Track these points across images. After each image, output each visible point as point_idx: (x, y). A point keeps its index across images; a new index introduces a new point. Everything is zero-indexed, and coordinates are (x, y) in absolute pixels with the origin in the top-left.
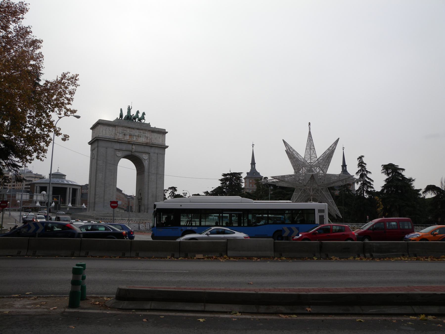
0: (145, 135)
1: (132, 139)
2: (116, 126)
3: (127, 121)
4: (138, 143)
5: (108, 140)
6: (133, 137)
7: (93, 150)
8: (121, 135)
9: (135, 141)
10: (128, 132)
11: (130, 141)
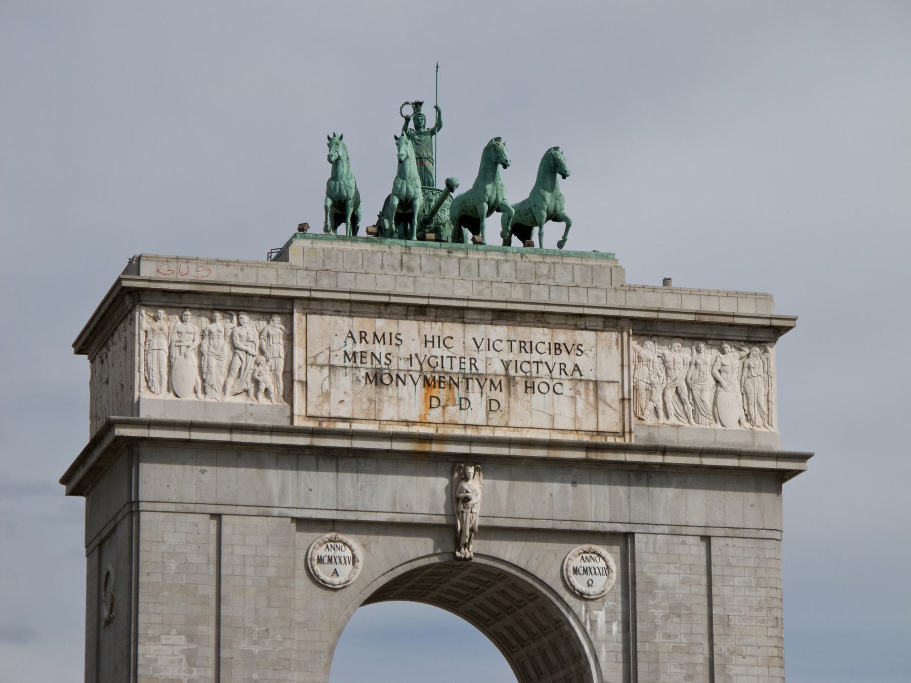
0: (563, 357)
1: (452, 410)
2: (292, 299)
3: (394, 248)
4: (510, 443)
5: (224, 437)
6: (459, 392)
7: (100, 545)
9: (486, 433)
11: (430, 430)
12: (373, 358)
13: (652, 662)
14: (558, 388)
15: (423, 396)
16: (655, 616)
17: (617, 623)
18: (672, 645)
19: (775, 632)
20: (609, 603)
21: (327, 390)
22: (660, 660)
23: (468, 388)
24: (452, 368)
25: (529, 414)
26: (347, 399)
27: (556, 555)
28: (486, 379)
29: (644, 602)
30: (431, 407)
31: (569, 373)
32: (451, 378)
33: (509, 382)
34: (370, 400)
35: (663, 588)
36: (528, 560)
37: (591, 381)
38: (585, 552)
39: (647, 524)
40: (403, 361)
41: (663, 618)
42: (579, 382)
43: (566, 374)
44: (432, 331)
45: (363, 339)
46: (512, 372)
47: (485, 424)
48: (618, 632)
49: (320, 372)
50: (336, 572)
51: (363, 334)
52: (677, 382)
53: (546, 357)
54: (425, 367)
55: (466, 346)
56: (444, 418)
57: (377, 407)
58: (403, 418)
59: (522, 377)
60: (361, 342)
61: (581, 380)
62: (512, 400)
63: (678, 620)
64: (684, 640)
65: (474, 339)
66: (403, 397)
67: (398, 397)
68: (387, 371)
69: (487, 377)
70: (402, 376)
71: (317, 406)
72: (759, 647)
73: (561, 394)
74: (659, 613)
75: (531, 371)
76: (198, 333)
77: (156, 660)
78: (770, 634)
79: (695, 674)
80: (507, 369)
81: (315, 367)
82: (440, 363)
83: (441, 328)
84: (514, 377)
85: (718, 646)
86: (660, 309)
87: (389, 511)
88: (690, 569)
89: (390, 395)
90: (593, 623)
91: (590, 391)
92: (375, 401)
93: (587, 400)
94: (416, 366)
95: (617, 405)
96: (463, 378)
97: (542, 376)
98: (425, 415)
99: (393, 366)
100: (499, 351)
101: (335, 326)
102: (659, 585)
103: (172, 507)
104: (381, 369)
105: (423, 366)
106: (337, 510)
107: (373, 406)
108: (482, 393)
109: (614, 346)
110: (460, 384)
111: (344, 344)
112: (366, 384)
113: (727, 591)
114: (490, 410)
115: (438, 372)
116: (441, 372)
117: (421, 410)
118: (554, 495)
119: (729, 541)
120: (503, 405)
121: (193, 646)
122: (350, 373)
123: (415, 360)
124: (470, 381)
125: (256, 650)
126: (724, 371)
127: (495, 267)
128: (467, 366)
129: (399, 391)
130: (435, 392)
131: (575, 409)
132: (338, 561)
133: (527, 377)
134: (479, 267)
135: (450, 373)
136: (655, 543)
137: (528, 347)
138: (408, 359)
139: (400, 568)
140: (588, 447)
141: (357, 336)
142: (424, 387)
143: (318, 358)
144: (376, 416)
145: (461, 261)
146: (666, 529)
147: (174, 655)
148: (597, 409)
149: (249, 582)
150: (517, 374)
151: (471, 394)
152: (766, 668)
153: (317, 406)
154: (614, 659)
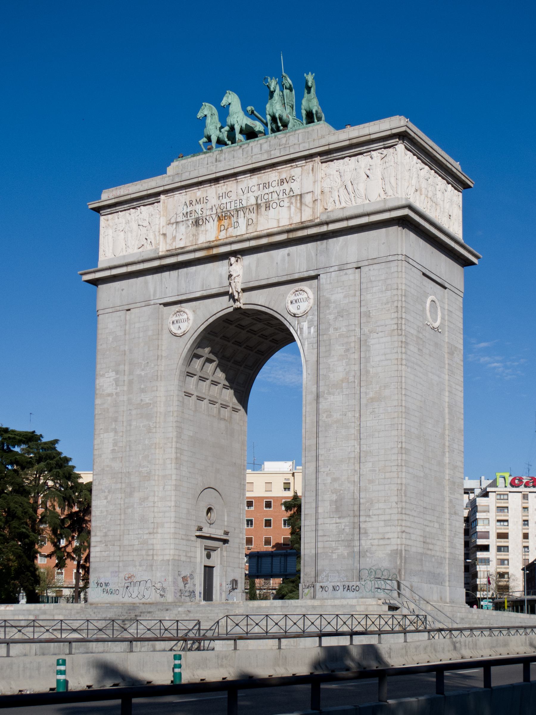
0: (286, 186)
1: (230, 230)
8: (182, 228)
10: (213, 201)
14: (282, 204)
19: (396, 315)
20: (310, 317)
25: (266, 221)
26: (183, 237)
27: (283, 296)
31: (287, 194)
32: (230, 213)
33: (258, 207)
34: (193, 235)
35: (334, 302)
37: (298, 195)
38: (297, 291)
40: (208, 210)
42: (292, 198)
46: (259, 202)
51: (191, 201)
52: (345, 183)
53: (277, 189)
54: (219, 211)
57: (197, 238)
58: (208, 240)
59: (264, 203)
61: (293, 196)
62: (259, 216)
63: (342, 319)
64: (345, 330)
68: (201, 218)
70: (208, 218)
72: (386, 326)
74: (331, 317)
75: (268, 199)
76: (124, 222)
77: (103, 386)
78: (392, 317)
80: (257, 201)
81: (170, 225)
82: (225, 207)
84: (260, 204)
89: (202, 230)
90: (301, 329)
93: (296, 207)
94: (214, 212)
95: (311, 205)
99: (204, 215)
102: (332, 301)
103: (110, 310)
104: (198, 218)
107: (194, 238)
109: (311, 172)
113: (369, 297)
119: (371, 267)
120: (254, 220)
121: (118, 376)
123: (214, 209)
124: (239, 212)
125: (143, 373)
127: (260, 148)
128: (238, 204)
132: (182, 321)
133: (266, 202)
134: (252, 150)
136: (330, 277)
137: (267, 186)
139: (210, 319)
140: (288, 231)
146: (336, 268)
147: (110, 382)
148: (301, 210)
150: (262, 202)
151: (239, 219)
152: (390, 337)
154: (312, 347)
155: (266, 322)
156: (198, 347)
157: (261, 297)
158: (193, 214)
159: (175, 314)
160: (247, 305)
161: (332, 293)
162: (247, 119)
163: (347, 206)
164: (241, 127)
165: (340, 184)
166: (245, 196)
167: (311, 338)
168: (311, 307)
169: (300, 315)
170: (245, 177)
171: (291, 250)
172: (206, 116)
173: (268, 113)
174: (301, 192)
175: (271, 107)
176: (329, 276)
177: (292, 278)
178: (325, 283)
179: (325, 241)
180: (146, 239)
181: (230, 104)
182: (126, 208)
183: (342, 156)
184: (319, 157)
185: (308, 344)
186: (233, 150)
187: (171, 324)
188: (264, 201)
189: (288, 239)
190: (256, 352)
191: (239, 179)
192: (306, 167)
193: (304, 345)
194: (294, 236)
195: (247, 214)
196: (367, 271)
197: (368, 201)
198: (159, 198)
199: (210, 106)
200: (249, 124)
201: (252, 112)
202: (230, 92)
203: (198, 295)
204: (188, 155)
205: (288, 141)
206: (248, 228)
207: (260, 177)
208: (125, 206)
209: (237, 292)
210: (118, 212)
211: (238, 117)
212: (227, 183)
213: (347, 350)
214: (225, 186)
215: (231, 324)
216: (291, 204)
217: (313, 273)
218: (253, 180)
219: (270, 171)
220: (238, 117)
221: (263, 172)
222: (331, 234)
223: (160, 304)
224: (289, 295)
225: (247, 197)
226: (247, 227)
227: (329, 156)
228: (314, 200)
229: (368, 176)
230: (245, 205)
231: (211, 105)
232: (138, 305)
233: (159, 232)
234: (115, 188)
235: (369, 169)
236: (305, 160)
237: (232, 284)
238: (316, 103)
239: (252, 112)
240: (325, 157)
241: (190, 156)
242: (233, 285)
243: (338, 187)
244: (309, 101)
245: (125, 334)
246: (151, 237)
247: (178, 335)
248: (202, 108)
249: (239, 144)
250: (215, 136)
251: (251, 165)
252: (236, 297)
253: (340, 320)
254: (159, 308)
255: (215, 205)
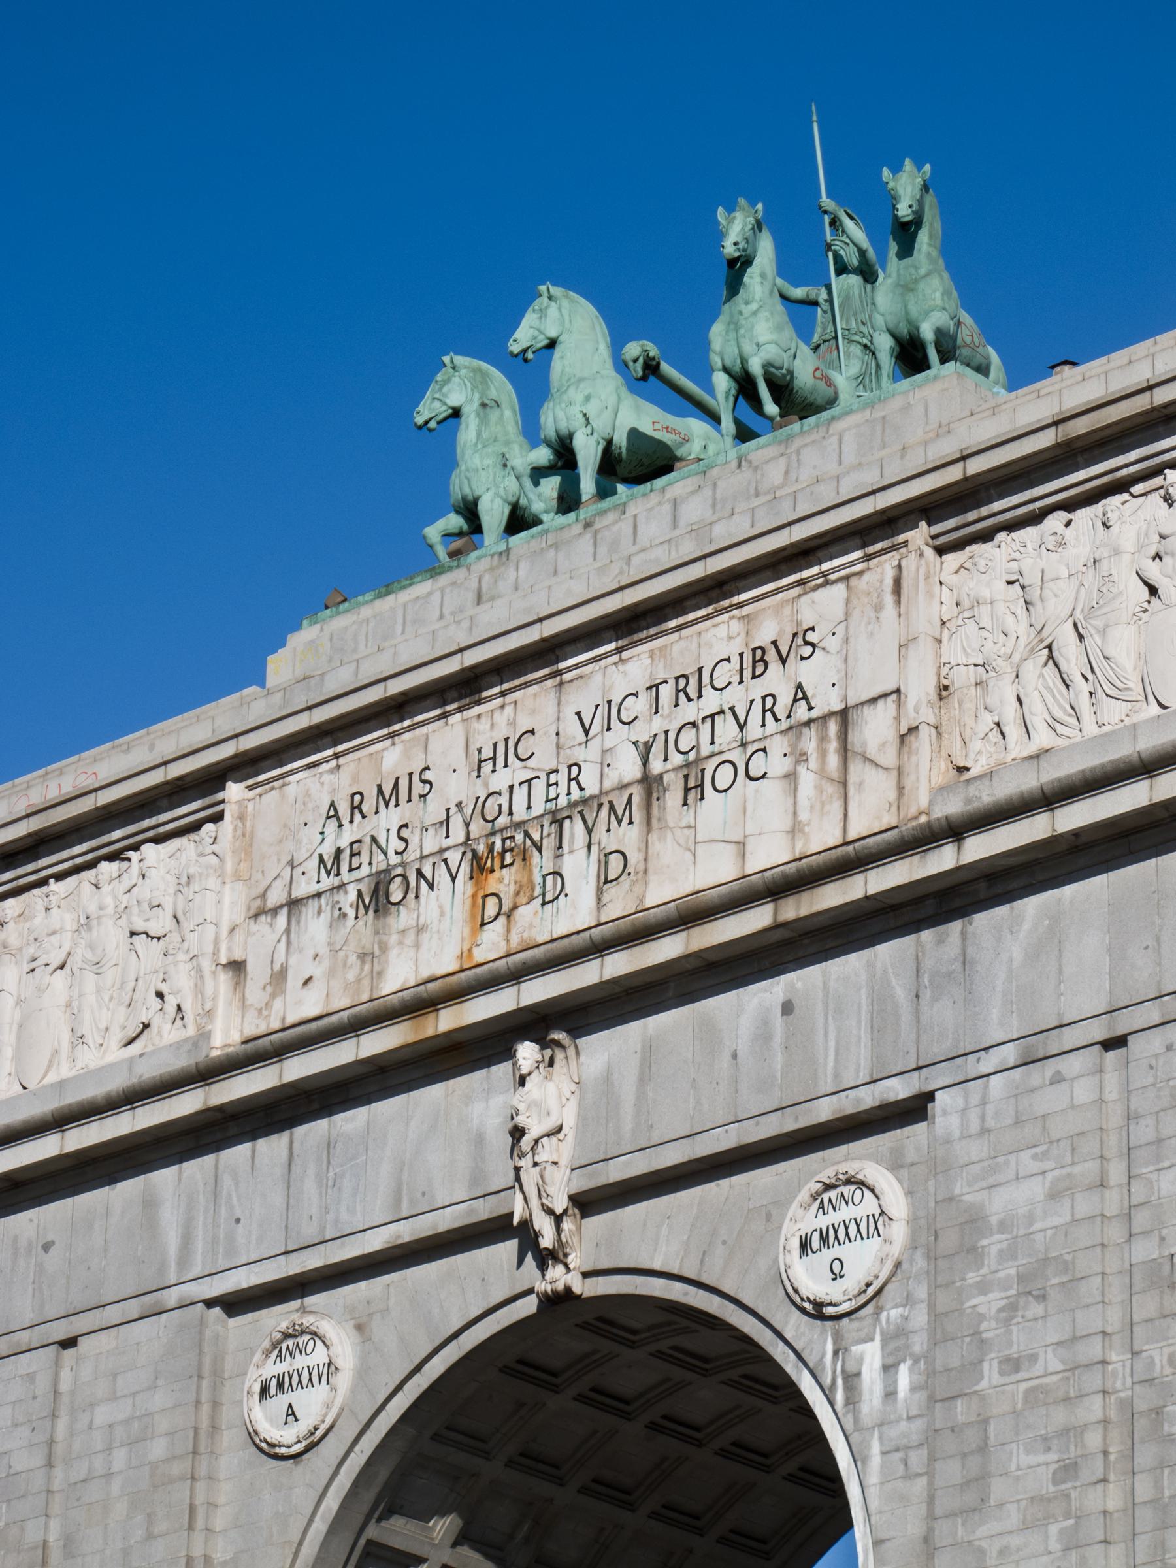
0: (777, 681)
1: (526, 913)
12: (374, 846)
13: (972, 1452)
15: (469, 902)
16: (980, 1314)
17: (909, 1362)
18: (1023, 1386)
20: (892, 1314)
21: (282, 964)
22: (992, 1441)
23: (560, 847)
24: (529, 808)
25: (688, 855)
26: (317, 971)
27: (768, 1217)
28: (600, 805)
29: (953, 1283)
30: (483, 924)
31: (781, 715)
33: (648, 794)
34: (363, 956)
35: (1003, 1227)
36: (704, 1253)
37: (832, 714)
38: (828, 1187)
39: (962, 1056)
40: (431, 831)
41: (1004, 1314)
42: (805, 730)
43: (777, 720)
44: (494, 734)
45: (356, 811)
47: (593, 924)
48: (913, 1389)
49: (271, 925)
50: (291, 1412)
51: (357, 798)
52: (1045, 633)
53: (736, 696)
55: (562, 740)
56: (508, 941)
57: (377, 968)
60: (351, 821)
61: (808, 723)
62: (653, 837)
65: (578, 714)
66: (429, 923)
67: (417, 926)
68: (399, 870)
69: (605, 800)
71: (260, 1011)
73: (764, 776)
74: (989, 1303)
79: (1082, 1456)
80: (645, 762)
81: (262, 918)
82: (505, 808)
83: (512, 716)
84: (661, 776)
85: (1144, 1354)
86: (965, 453)
87: (387, 1221)
88: (1073, 1149)
89: (401, 928)
90: (852, 1379)
91: (829, 742)
92: (373, 953)
93: (822, 773)
94: (458, 834)
95: (889, 758)
96: (551, 823)
97: (724, 747)
98: (470, 950)
99: (412, 855)
100: (629, 723)
101: (304, 804)
102: (994, 1220)
104: (387, 871)
105: (472, 827)
106: (286, 1253)
107: (367, 967)
108: (589, 846)
109: (889, 599)
110: (545, 842)
111: (320, 837)
112: (356, 918)
114: (606, 882)
115: (501, 830)
116: (506, 828)
117: (463, 940)
118: (740, 1054)
120: (634, 857)
122: (327, 905)
123: (457, 823)
124: (567, 823)
126: (1166, 554)
127: (669, 518)
129: (422, 910)
130: (492, 883)
131: (795, 803)
132: (305, 1381)
133: (688, 765)
135: (524, 822)
136: (984, 1103)
137: (692, 690)
138: (441, 823)
141: (344, 809)
142: (471, 878)
143: (269, 893)
144: (372, 990)
145: (599, 537)
146: (1009, 1054)
148: (845, 784)
149: (116, 1487)
150: (669, 766)
151: (566, 858)
153: (260, 1011)
154: (901, 1469)
155: (734, 1374)
156: (389, 1512)
157: (664, 1230)
158: (364, 857)
159: (276, 1345)
160: (601, 1279)
161: (991, 1181)
162: (638, 408)
163: (1061, 742)
164: (609, 442)
165: (1023, 641)
166: (595, 744)
167: (898, 1421)
168: (898, 1265)
169: (845, 1307)
170: (595, 660)
171: (799, 985)
172: (456, 413)
173: (717, 362)
174: (845, 698)
175: (732, 335)
176: (975, 1099)
177: (803, 1123)
178: (957, 1134)
179: (956, 926)
180: (160, 995)
181: (552, 344)
182: (79, 861)
183: (1031, 507)
184: (923, 524)
185: (883, 1453)
186: (556, 546)
187: (257, 1397)
188: (677, 759)
189: (777, 926)
190: (722, 1540)
191: (569, 669)
192: (866, 577)
193: (864, 1463)
194: (804, 912)
195: (600, 832)
196: (1156, 1056)
197: (1155, 710)
198: (220, 796)
199: (479, 370)
200: (646, 428)
201: (651, 368)
202: (555, 290)
203: (374, 1242)
204: (363, 593)
205: (793, 475)
206: (606, 898)
207: (662, 649)
208: (77, 850)
209: (549, 1211)
210: (43, 882)
211: (588, 399)
212: (517, 695)
213: (1068, 1470)
214: (509, 710)
215: (555, 1389)
216: (798, 762)
217: (899, 1089)
218: (630, 667)
219: (707, 617)
220: (588, 399)
221: (672, 623)
222: (982, 885)
223: (210, 1303)
224: (794, 1209)
225: (604, 752)
226: (600, 892)
227: (972, 516)
228: (904, 730)
229: (1153, 591)
230: (591, 788)
231: (484, 365)
232: (113, 1314)
233: (216, 953)
234: (41, 772)
235: (1158, 556)
236: (864, 546)
237: (523, 1174)
238: (938, 295)
239: (651, 368)
240: (951, 523)
241: (369, 596)
242: (530, 1177)
243: (1016, 657)
244: (906, 288)
245: (50, 1465)
246: (182, 985)
247: (283, 1451)
248: (439, 377)
249: (582, 516)
250: (498, 501)
251: (618, 596)
252: (547, 1241)
253: (1029, 1314)
254: (202, 1323)
255: (459, 805)
